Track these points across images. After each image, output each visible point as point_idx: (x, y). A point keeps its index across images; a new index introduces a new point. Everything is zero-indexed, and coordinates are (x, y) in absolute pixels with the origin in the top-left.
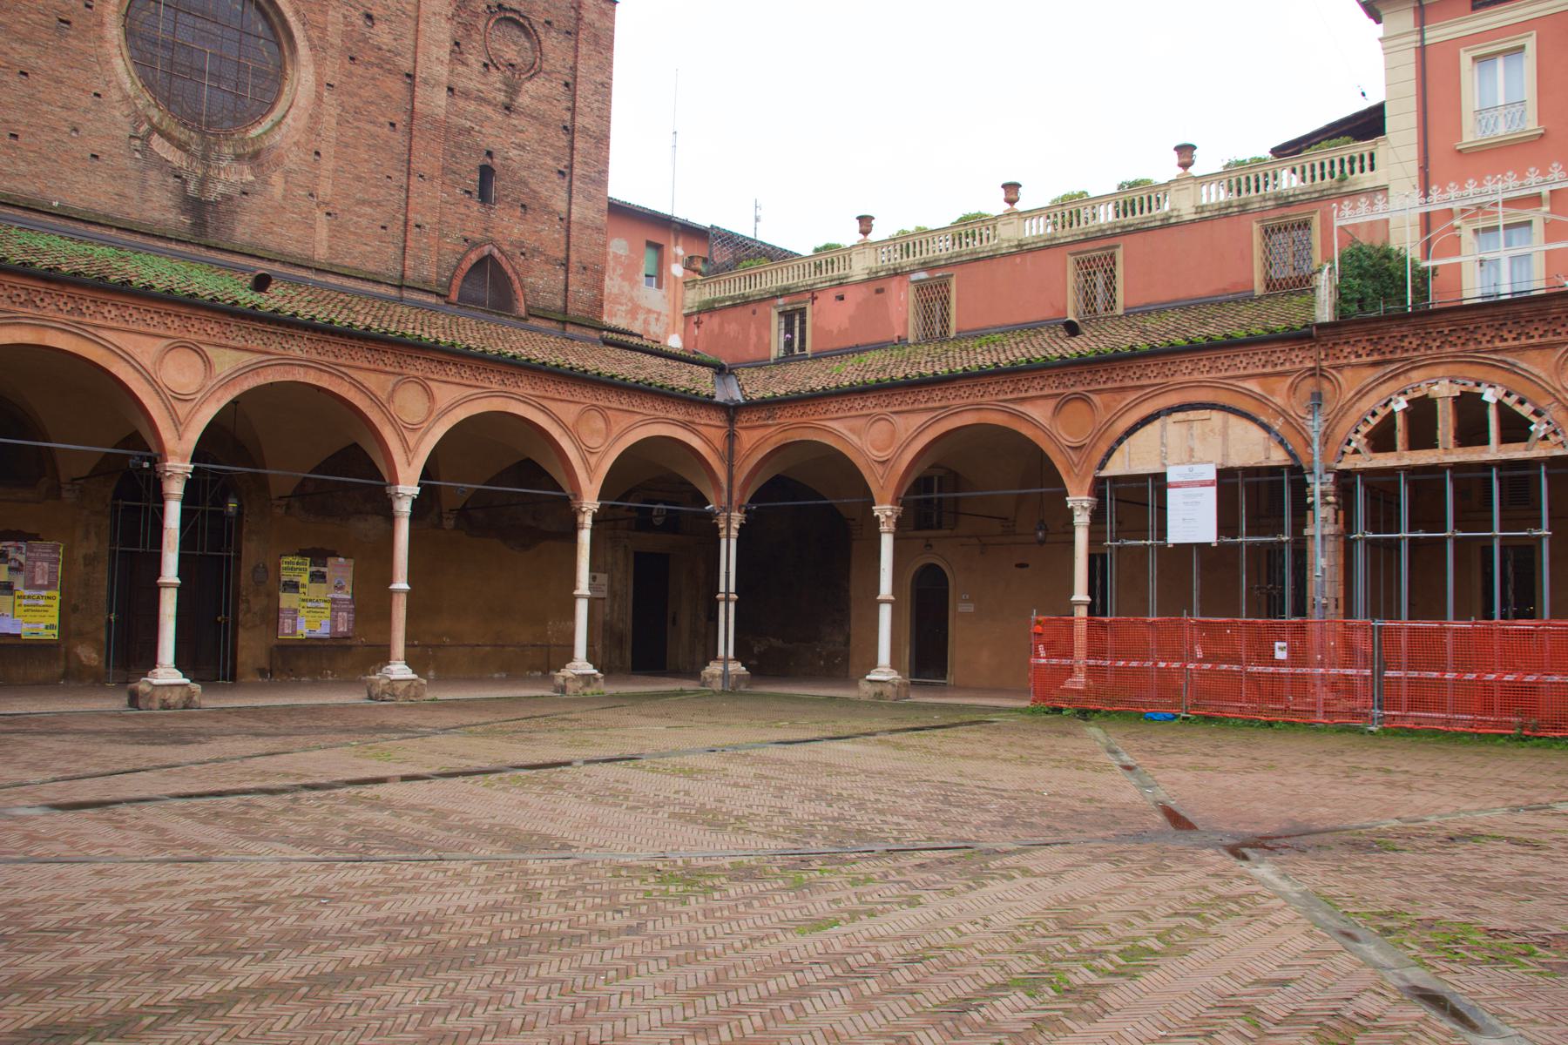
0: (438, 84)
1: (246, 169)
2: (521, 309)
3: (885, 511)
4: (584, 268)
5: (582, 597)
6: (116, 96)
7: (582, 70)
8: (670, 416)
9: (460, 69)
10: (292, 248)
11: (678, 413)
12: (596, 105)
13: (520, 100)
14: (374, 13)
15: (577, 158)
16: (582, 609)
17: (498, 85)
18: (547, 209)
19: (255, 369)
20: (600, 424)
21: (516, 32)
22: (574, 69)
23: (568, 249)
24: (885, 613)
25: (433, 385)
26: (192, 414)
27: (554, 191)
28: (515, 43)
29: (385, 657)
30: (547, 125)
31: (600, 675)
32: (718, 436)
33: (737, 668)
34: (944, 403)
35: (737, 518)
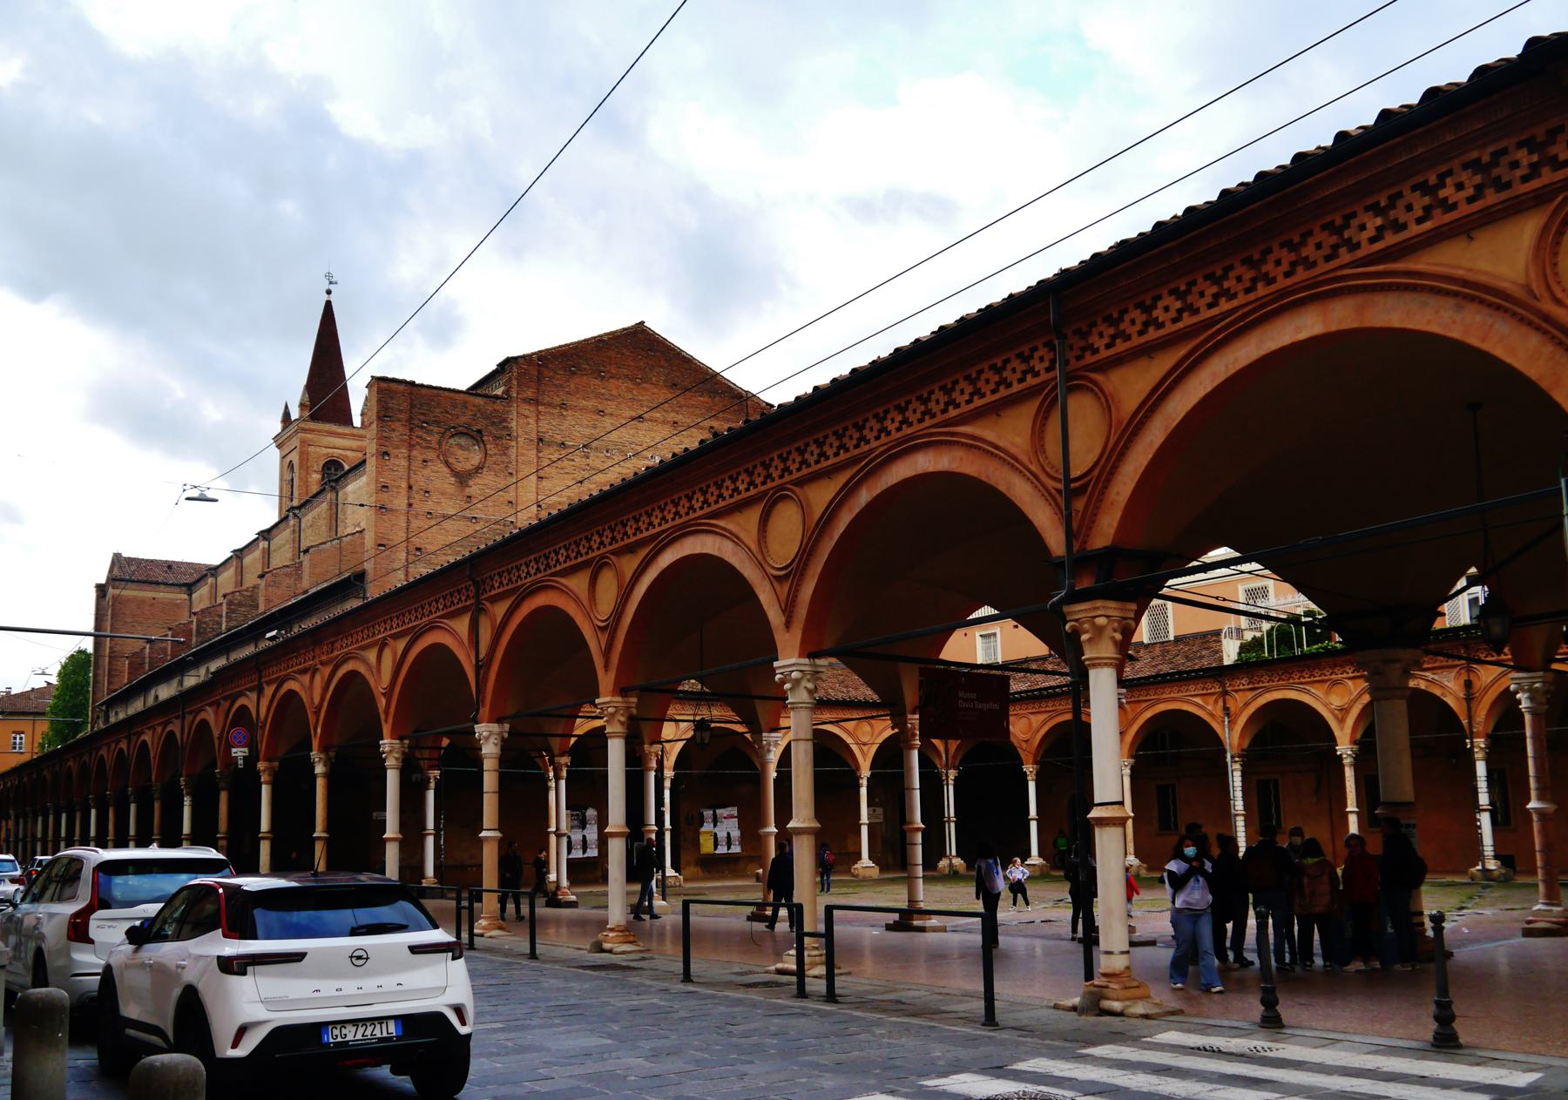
3: (1029, 769)
5: (864, 824)
16: (864, 831)
20: (868, 728)
24: (1034, 826)
33: (958, 862)
34: (1054, 708)
35: (952, 774)
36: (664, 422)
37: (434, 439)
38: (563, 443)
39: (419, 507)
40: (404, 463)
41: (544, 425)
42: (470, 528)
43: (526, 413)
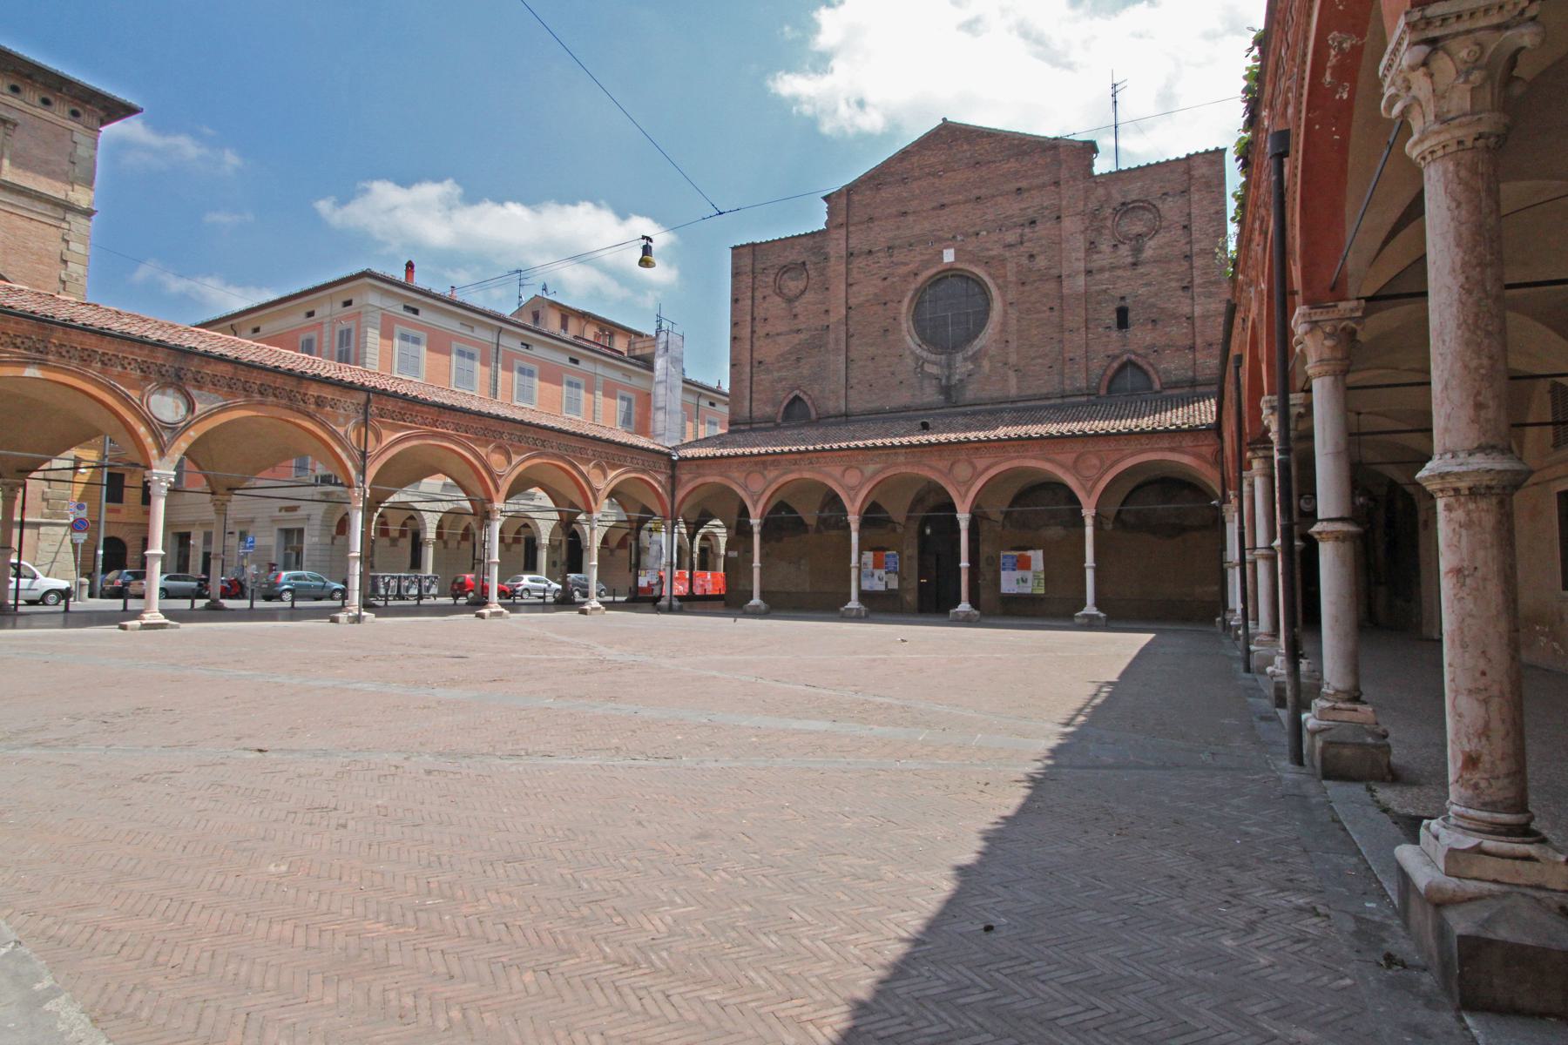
0: (1078, 273)
1: (969, 363)
2: (1157, 386)
4: (1210, 345)
6: (908, 352)
7: (1195, 211)
8: (1156, 446)
9: (1095, 257)
10: (995, 395)
11: (1166, 443)
12: (1211, 230)
13: (1144, 255)
14: (1035, 252)
15: (1196, 273)
16: (1090, 576)
17: (1126, 253)
18: (1174, 316)
19: (883, 469)
20: (1095, 461)
21: (1141, 212)
22: (1189, 214)
23: (1194, 336)
25: (975, 460)
26: (856, 494)
27: (1180, 302)
28: (1140, 220)
29: (958, 602)
30: (1169, 262)
31: (1102, 615)
32: (1207, 450)
36: (966, 202)
37: (770, 280)
38: (870, 251)
39: (761, 331)
40: (750, 302)
41: (853, 242)
42: (796, 339)
43: (836, 236)
